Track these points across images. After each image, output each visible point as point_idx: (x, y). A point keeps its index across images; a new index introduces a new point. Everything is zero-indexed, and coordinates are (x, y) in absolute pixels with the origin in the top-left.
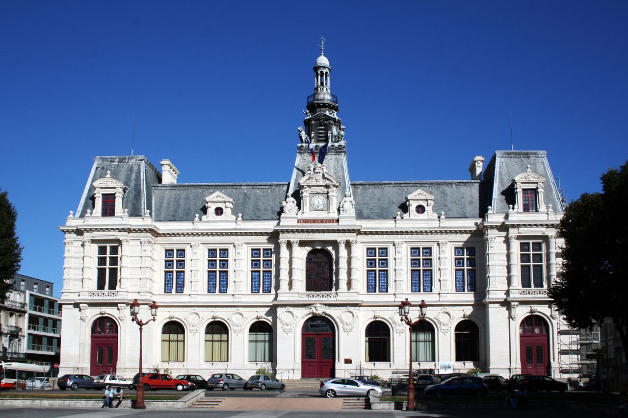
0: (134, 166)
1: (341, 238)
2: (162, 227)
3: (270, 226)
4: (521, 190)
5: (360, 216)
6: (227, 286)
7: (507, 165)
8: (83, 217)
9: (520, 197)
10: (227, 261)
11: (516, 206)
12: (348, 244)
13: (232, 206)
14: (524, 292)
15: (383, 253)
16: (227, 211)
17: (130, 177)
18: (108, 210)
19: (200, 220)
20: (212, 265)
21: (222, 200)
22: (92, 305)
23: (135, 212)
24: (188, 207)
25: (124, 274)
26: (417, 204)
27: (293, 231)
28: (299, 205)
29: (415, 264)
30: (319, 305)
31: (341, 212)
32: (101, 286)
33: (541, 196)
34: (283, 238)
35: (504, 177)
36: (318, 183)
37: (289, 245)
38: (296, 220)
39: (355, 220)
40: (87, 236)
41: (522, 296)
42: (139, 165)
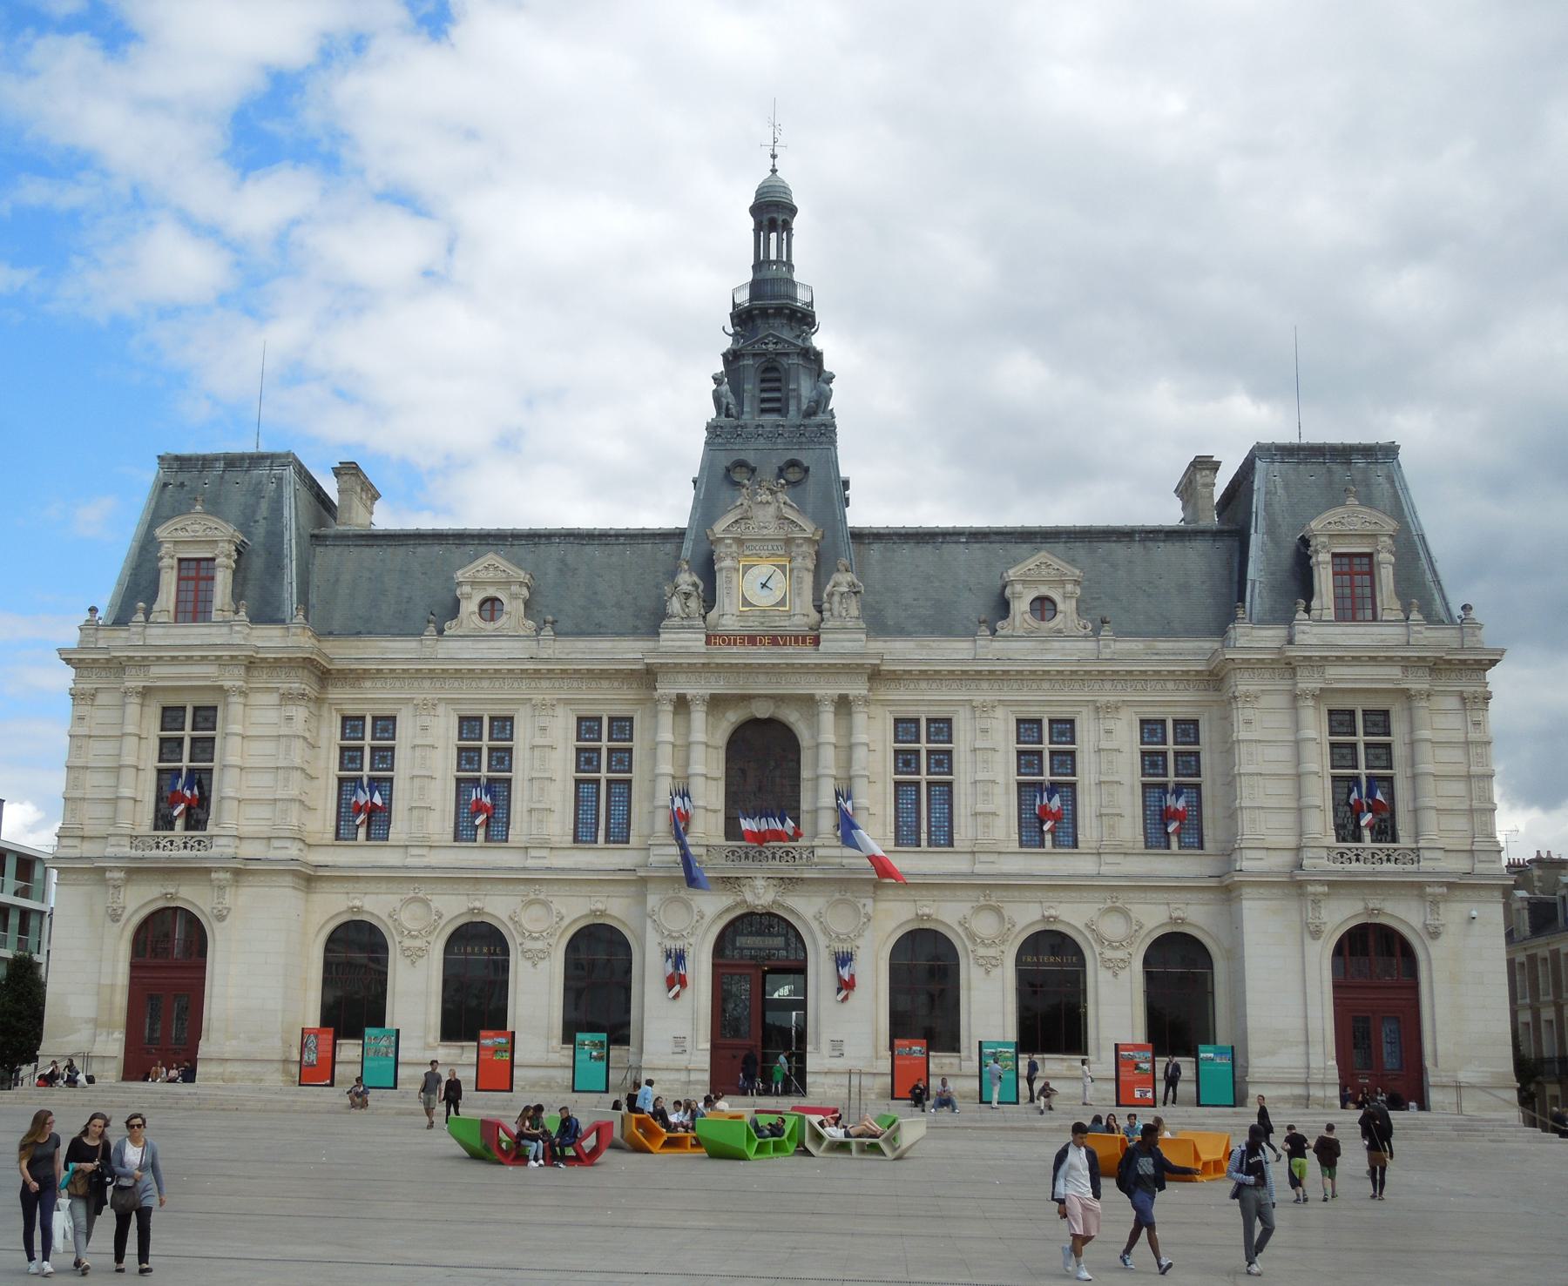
0: (264, 480)
1: (826, 690)
2: (343, 652)
3: (630, 651)
4: (1328, 557)
5: (877, 626)
6: (508, 824)
7: (1286, 487)
8: (126, 624)
9: (1324, 579)
10: (509, 750)
11: (1315, 603)
12: (844, 705)
13: (525, 592)
14: (1342, 855)
15: (939, 732)
16: (513, 608)
17: (254, 512)
18: (194, 608)
19: (441, 632)
20: (470, 761)
21: (501, 576)
22: (137, 872)
23: (265, 613)
24: (406, 594)
25: (225, 786)
26: (1035, 594)
27: (691, 669)
28: (709, 601)
29: (1029, 765)
30: (763, 882)
31: (826, 614)
32: (163, 821)
33: (1386, 576)
34: (667, 689)
35: (1280, 520)
36: (765, 532)
37: (682, 704)
38: (703, 637)
39: (863, 637)
40: (134, 681)
41: (1338, 866)
42: (280, 479)
